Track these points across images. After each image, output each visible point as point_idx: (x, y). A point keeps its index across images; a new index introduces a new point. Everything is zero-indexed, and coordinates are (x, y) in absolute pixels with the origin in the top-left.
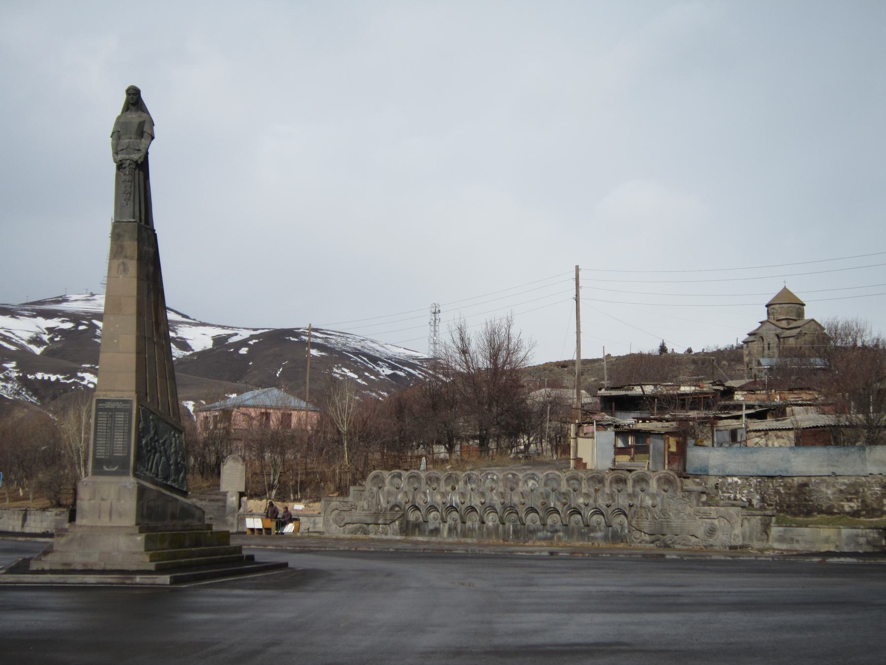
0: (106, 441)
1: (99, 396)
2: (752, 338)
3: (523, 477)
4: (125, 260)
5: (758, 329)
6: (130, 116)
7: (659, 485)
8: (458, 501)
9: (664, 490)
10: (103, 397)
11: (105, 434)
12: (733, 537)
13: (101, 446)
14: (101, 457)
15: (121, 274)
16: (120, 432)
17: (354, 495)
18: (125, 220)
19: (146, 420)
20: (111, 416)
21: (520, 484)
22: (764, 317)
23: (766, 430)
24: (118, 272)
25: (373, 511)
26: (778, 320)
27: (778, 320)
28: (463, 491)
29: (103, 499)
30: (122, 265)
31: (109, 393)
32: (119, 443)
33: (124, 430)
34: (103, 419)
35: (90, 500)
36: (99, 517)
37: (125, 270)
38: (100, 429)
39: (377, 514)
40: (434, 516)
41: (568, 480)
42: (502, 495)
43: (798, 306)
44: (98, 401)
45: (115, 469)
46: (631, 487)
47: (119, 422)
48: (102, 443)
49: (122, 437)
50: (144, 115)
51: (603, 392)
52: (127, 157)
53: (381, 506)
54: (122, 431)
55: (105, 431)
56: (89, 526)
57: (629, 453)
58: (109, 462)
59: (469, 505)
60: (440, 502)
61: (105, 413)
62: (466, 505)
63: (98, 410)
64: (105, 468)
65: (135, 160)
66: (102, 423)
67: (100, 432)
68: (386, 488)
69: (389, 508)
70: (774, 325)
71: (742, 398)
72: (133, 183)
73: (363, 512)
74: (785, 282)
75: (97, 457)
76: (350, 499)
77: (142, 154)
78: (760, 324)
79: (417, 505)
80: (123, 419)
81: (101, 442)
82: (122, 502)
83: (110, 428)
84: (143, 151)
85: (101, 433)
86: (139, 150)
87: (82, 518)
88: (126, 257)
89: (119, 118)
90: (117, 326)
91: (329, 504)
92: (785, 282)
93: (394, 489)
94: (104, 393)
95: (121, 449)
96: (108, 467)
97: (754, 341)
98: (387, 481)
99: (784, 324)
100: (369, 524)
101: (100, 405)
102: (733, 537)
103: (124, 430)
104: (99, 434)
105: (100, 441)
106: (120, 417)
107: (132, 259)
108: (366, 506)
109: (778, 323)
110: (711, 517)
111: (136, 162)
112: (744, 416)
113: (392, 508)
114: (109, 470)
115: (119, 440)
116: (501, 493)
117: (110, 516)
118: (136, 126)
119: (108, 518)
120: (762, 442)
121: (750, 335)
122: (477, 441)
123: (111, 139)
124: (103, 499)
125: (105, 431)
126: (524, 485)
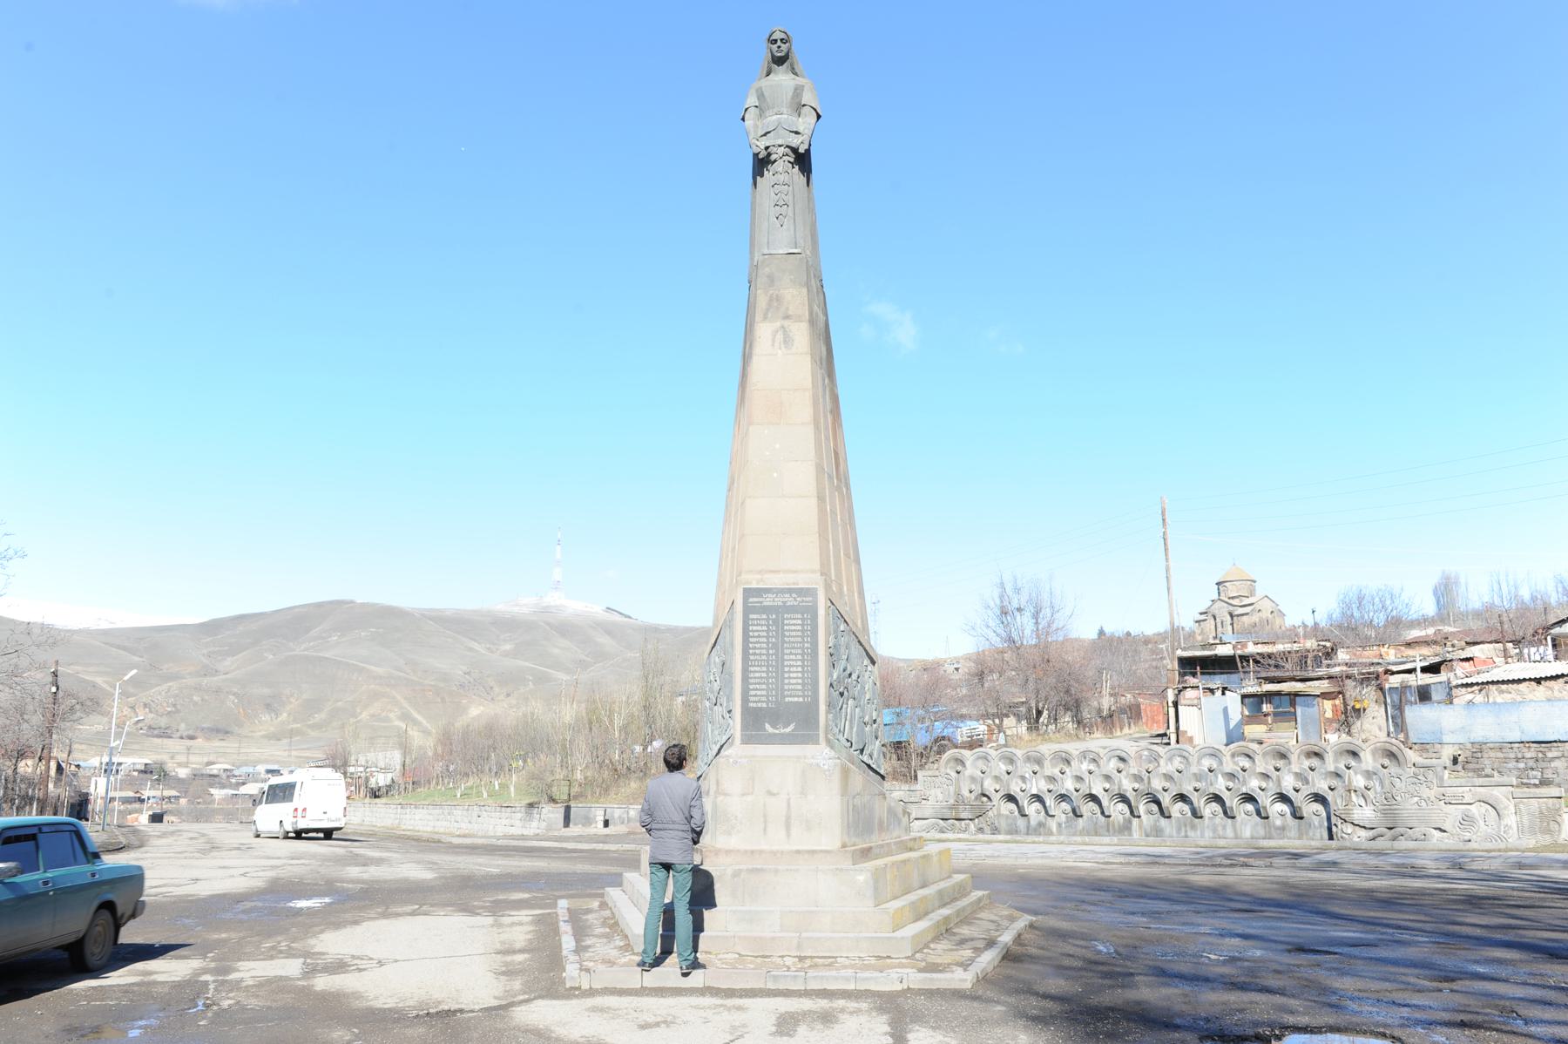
0: (767, 672)
1: (751, 583)
2: (1203, 617)
3: (1165, 753)
4: (786, 323)
5: (1209, 608)
6: (776, 79)
7: (1375, 760)
9: (1383, 766)
10: (758, 583)
12: (1503, 830)
13: (759, 684)
14: (759, 705)
15: (780, 349)
16: (796, 654)
18: (781, 252)
20: (775, 622)
21: (1162, 762)
22: (1216, 596)
23: (1483, 683)
24: (773, 345)
25: (952, 801)
26: (1233, 598)
27: (1229, 598)
29: (770, 793)
30: (780, 333)
32: (795, 675)
35: (743, 795)
36: (765, 830)
37: (787, 341)
38: (755, 648)
41: (1233, 756)
43: (1249, 582)
44: (748, 593)
45: (788, 730)
46: (1331, 761)
47: (792, 634)
48: (761, 678)
51: (1180, 653)
54: (799, 651)
55: (764, 652)
56: (746, 852)
58: (776, 714)
59: (1088, 792)
61: (764, 616)
63: (747, 610)
65: (794, 145)
66: (759, 636)
67: (755, 654)
69: (973, 798)
71: (1348, 657)
72: (791, 188)
75: (751, 705)
76: (918, 787)
77: (805, 138)
78: (1211, 603)
80: (799, 628)
81: (757, 675)
83: (775, 646)
85: (758, 657)
86: (797, 133)
88: (787, 317)
90: (777, 446)
94: (759, 577)
95: (800, 687)
97: (1205, 620)
100: (946, 819)
101: (751, 600)
102: (1503, 830)
103: (803, 649)
104: (752, 657)
105: (755, 672)
106: (794, 624)
107: (799, 319)
108: (940, 797)
109: (1231, 601)
110: (1465, 802)
111: (795, 150)
112: (1419, 670)
113: (976, 798)
114: (777, 732)
120: (1479, 698)
121: (1201, 614)
122: (1004, 719)
124: (770, 793)
125: (764, 652)
126: (1167, 764)
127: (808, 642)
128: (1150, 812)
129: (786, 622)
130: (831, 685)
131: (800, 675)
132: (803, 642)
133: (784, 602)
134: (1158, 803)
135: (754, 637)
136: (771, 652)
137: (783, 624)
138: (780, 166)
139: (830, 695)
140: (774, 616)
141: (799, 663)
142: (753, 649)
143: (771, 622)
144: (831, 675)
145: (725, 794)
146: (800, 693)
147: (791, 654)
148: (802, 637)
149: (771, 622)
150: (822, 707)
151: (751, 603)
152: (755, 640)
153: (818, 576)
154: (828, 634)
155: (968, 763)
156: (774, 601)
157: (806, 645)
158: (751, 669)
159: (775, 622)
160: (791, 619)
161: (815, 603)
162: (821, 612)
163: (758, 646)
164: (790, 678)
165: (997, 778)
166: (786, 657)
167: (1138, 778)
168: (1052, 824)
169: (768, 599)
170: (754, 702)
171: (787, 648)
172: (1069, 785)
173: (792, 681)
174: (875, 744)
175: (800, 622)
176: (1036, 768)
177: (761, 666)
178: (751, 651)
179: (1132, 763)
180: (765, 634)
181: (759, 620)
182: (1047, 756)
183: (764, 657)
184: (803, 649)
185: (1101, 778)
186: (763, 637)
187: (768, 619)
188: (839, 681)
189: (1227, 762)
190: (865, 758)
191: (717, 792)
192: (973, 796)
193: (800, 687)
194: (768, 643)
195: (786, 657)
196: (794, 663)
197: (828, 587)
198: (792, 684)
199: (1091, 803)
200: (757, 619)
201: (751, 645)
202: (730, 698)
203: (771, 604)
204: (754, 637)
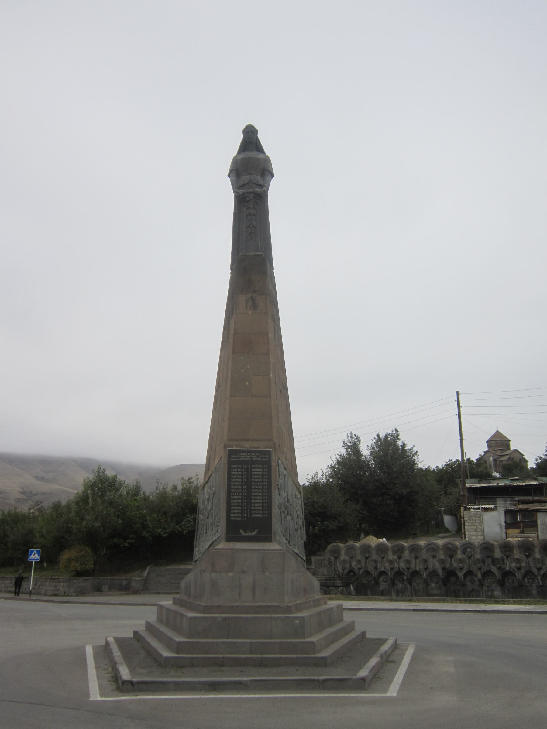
0: (242, 499)
8: (405, 567)
11: (240, 491)
13: (237, 506)
14: (237, 519)
17: (315, 563)
18: (251, 254)
22: (486, 449)
24: (246, 308)
28: (409, 559)
29: (243, 572)
32: (257, 501)
34: (237, 473)
38: (235, 485)
40: (383, 579)
42: (442, 561)
44: (231, 453)
45: (254, 534)
47: (257, 477)
48: (238, 503)
49: (261, 494)
52: (251, 190)
53: (339, 572)
54: (261, 487)
55: (240, 487)
57: (519, 528)
60: (389, 568)
61: (240, 466)
62: (411, 571)
63: (230, 463)
66: (237, 478)
67: (234, 489)
69: (345, 573)
70: (493, 453)
73: (324, 577)
74: (497, 427)
75: (232, 519)
79: (369, 570)
80: (261, 473)
81: (236, 501)
82: (267, 574)
88: (254, 292)
89: (235, 158)
90: (249, 366)
92: (497, 427)
93: (347, 558)
94: (237, 443)
95: (261, 508)
96: (245, 532)
98: (343, 552)
99: (499, 453)
101: (232, 456)
103: (263, 486)
105: (234, 499)
106: (257, 471)
108: (326, 573)
114: (247, 534)
115: (258, 498)
116: (442, 560)
117: (254, 593)
123: (229, 179)
124: (243, 572)
127: (265, 482)
129: (253, 470)
131: (261, 501)
132: (263, 482)
133: (252, 458)
135: (234, 478)
136: (244, 487)
137: (251, 471)
140: (246, 466)
141: (261, 494)
142: (233, 485)
143: (244, 470)
146: (261, 512)
147: (256, 489)
148: (263, 479)
149: (244, 470)
151: (233, 458)
152: (236, 480)
156: (246, 457)
157: (265, 483)
158: (232, 497)
160: (256, 468)
163: (236, 483)
164: (255, 503)
166: (253, 491)
169: (242, 456)
170: (233, 517)
171: (253, 485)
173: (257, 505)
175: (261, 470)
177: (238, 496)
178: (232, 487)
180: (240, 477)
181: (238, 468)
183: (240, 491)
184: (263, 486)
186: (239, 478)
187: (242, 468)
193: (261, 508)
194: (242, 482)
195: (253, 491)
196: (257, 494)
198: (257, 507)
200: (236, 468)
201: (232, 483)
203: (244, 459)
204: (234, 478)
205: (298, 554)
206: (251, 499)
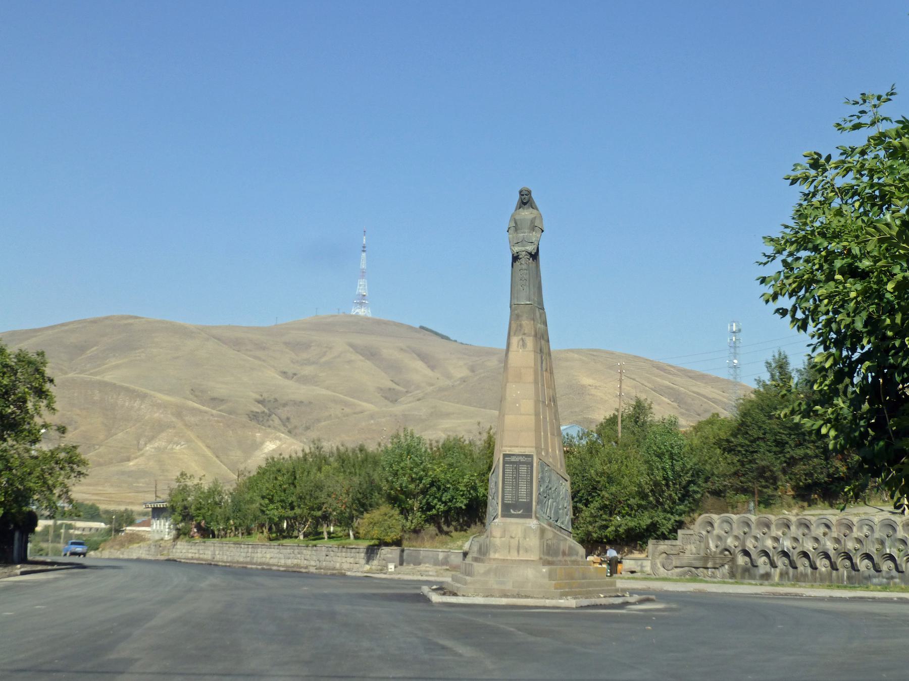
0: (512, 489)
4: (524, 337)
8: (790, 547)
19: (542, 472)
20: (516, 468)
21: (855, 529)
24: (518, 347)
25: (702, 554)
29: (512, 537)
31: (513, 448)
33: (527, 479)
35: (501, 537)
36: (509, 551)
37: (524, 345)
39: (706, 558)
44: (505, 456)
45: (520, 512)
50: (534, 211)
52: (523, 249)
56: (501, 559)
58: (515, 506)
63: (505, 463)
64: (512, 511)
68: (716, 532)
75: (505, 502)
76: (678, 542)
77: (535, 246)
82: (528, 539)
83: (515, 478)
84: (536, 243)
87: (495, 552)
88: (524, 334)
91: (657, 547)
94: (509, 448)
101: (507, 458)
103: (527, 479)
106: (523, 469)
107: (529, 336)
108: (694, 550)
111: (530, 254)
113: (722, 552)
118: (529, 223)
119: (516, 553)
128: (845, 567)
130: (539, 494)
134: (849, 558)
138: (523, 261)
139: (538, 498)
144: (539, 489)
145: (494, 537)
150: (534, 503)
153: (534, 449)
154: (538, 473)
155: (716, 525)
159: (516, 468)
161: (532, 460)
162: (535, 465)
165: (737, 538)
167: (837, 541)
168: (776, 573)
172: (787, 544)
174: (565, 518)
176: (765, 530)
179: (834, 529)
182: (773, 522)
185: (812, 540)
188: (543, 492)
189: (900, 531)
190: (559, 524)
191: (491, 537)
192: (718, 551)
197: (539, 453)
199: (804, 559)
202: (498, 498)
205: (561, 527)
206: (518, 489)
